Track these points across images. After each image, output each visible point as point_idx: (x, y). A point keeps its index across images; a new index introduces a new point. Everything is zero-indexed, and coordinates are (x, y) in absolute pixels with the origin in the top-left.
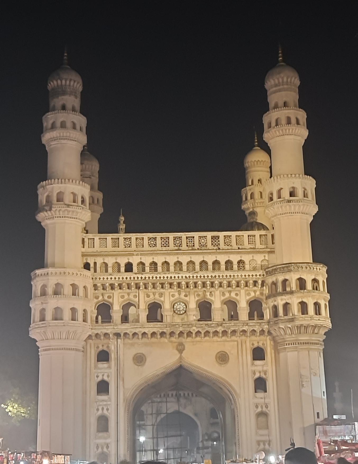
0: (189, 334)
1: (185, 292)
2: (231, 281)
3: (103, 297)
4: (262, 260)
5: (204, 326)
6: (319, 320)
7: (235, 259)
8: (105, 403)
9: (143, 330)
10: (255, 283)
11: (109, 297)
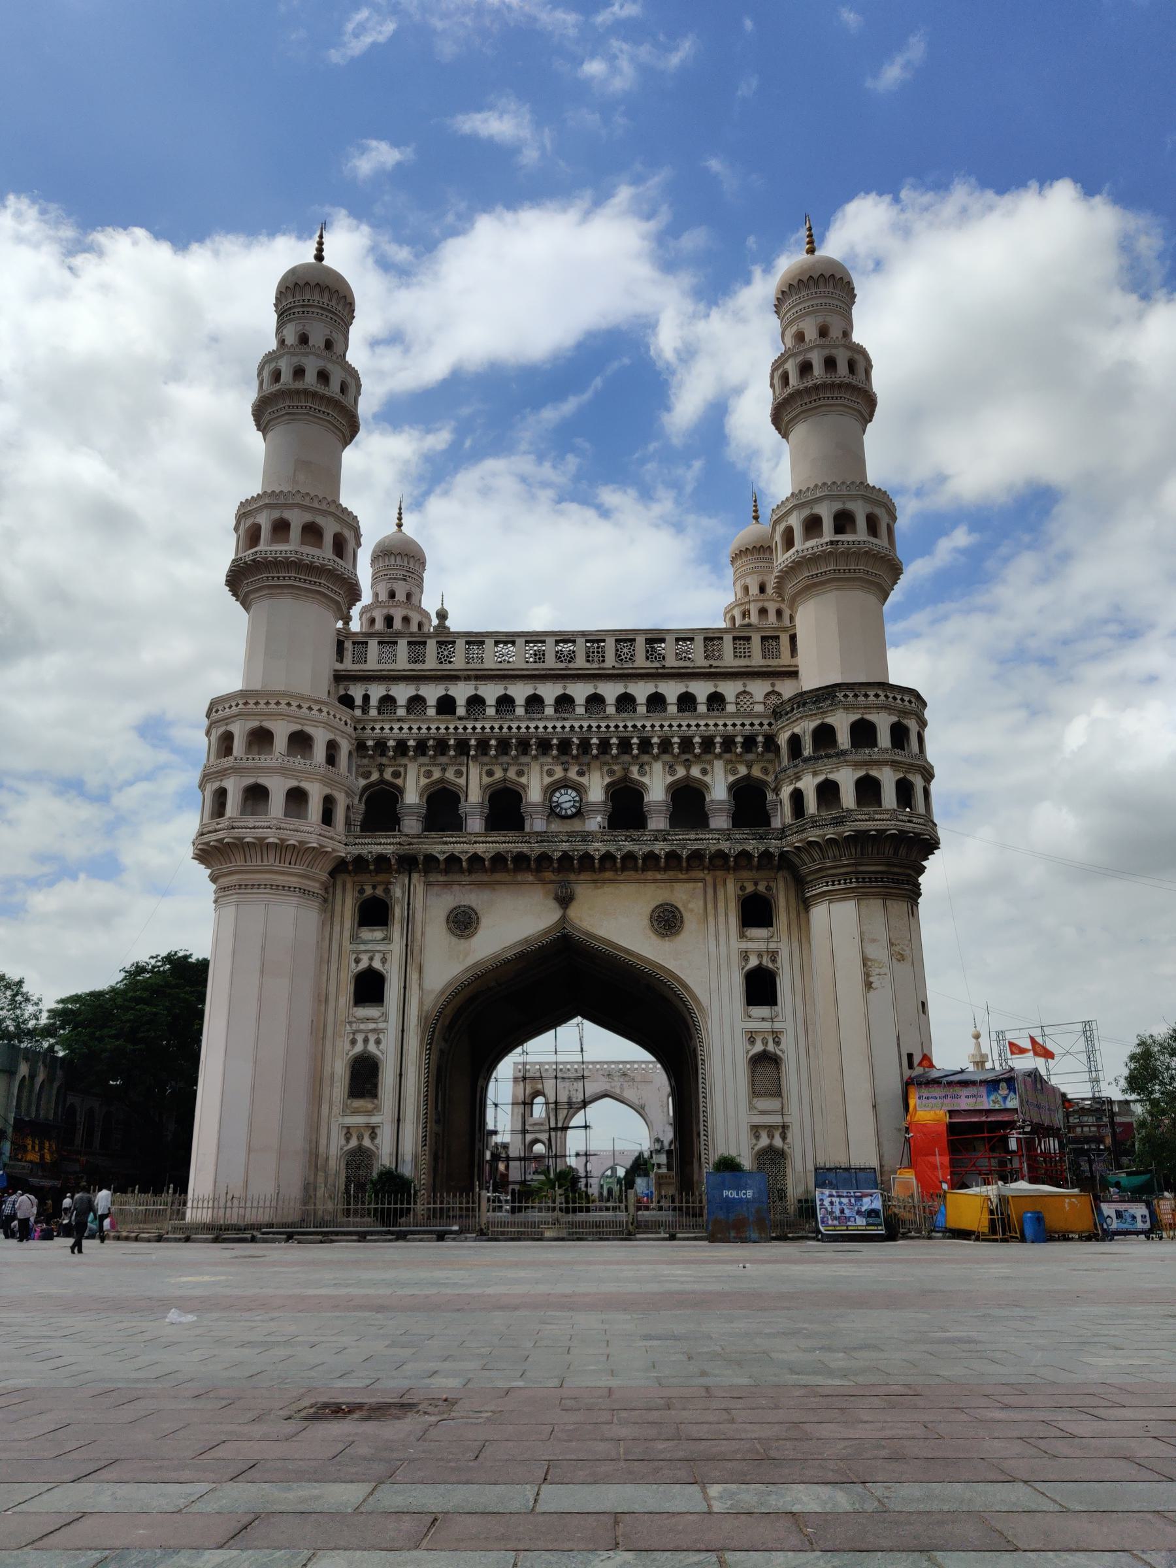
0: (587, 858)
1: (580, 765)
3: (381, 775)
4: (768, 694)
5: (623, 844)
6: (909, 821)
7: (701, 690)
8: (372, 1026)
10: (750, 742)
11: (396, 775)
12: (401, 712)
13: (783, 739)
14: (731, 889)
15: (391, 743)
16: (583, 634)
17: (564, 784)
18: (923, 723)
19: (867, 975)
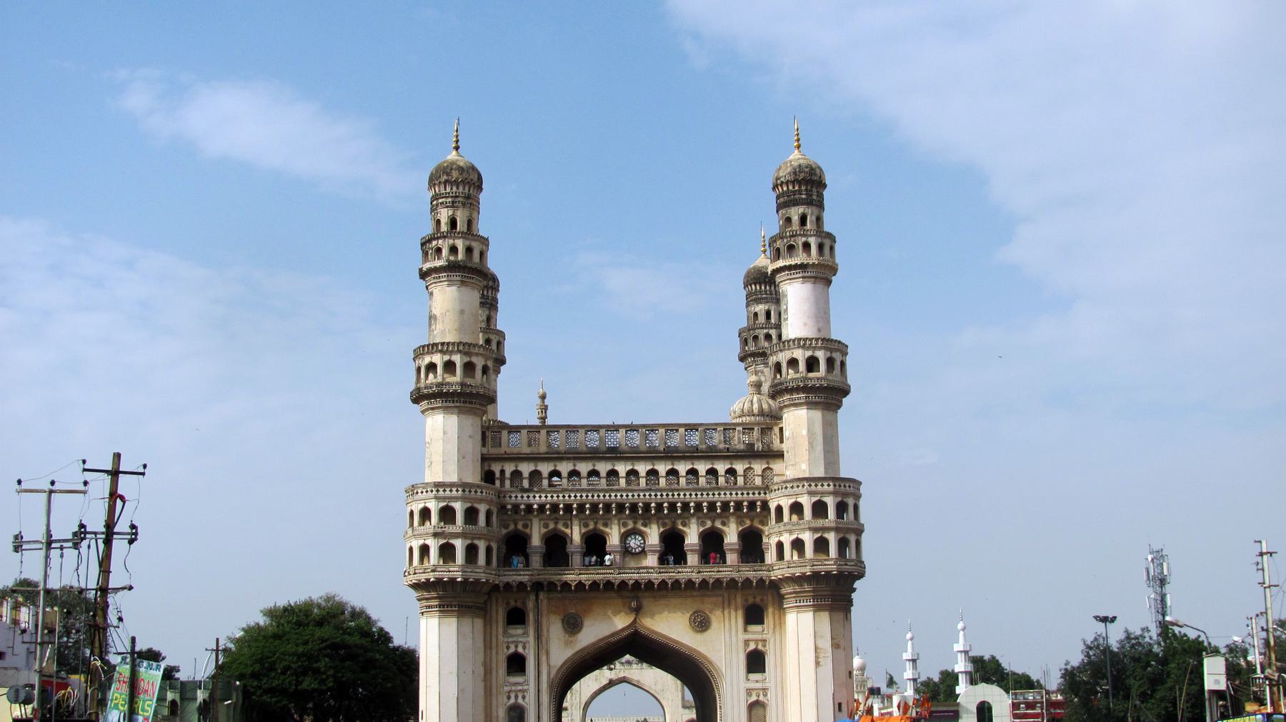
0: (650, 584)
2: (714, 503)
4: (764, 470)
9: (578, 578)
10: (752, 505)
11: (525, 526)
12: (526, 484)
13: (773, 505)
14: (739, 600)
15: (522, 507)
16: (644, 426)
17: (635, 532)
18: (857, 497)
19: (817, 657)
